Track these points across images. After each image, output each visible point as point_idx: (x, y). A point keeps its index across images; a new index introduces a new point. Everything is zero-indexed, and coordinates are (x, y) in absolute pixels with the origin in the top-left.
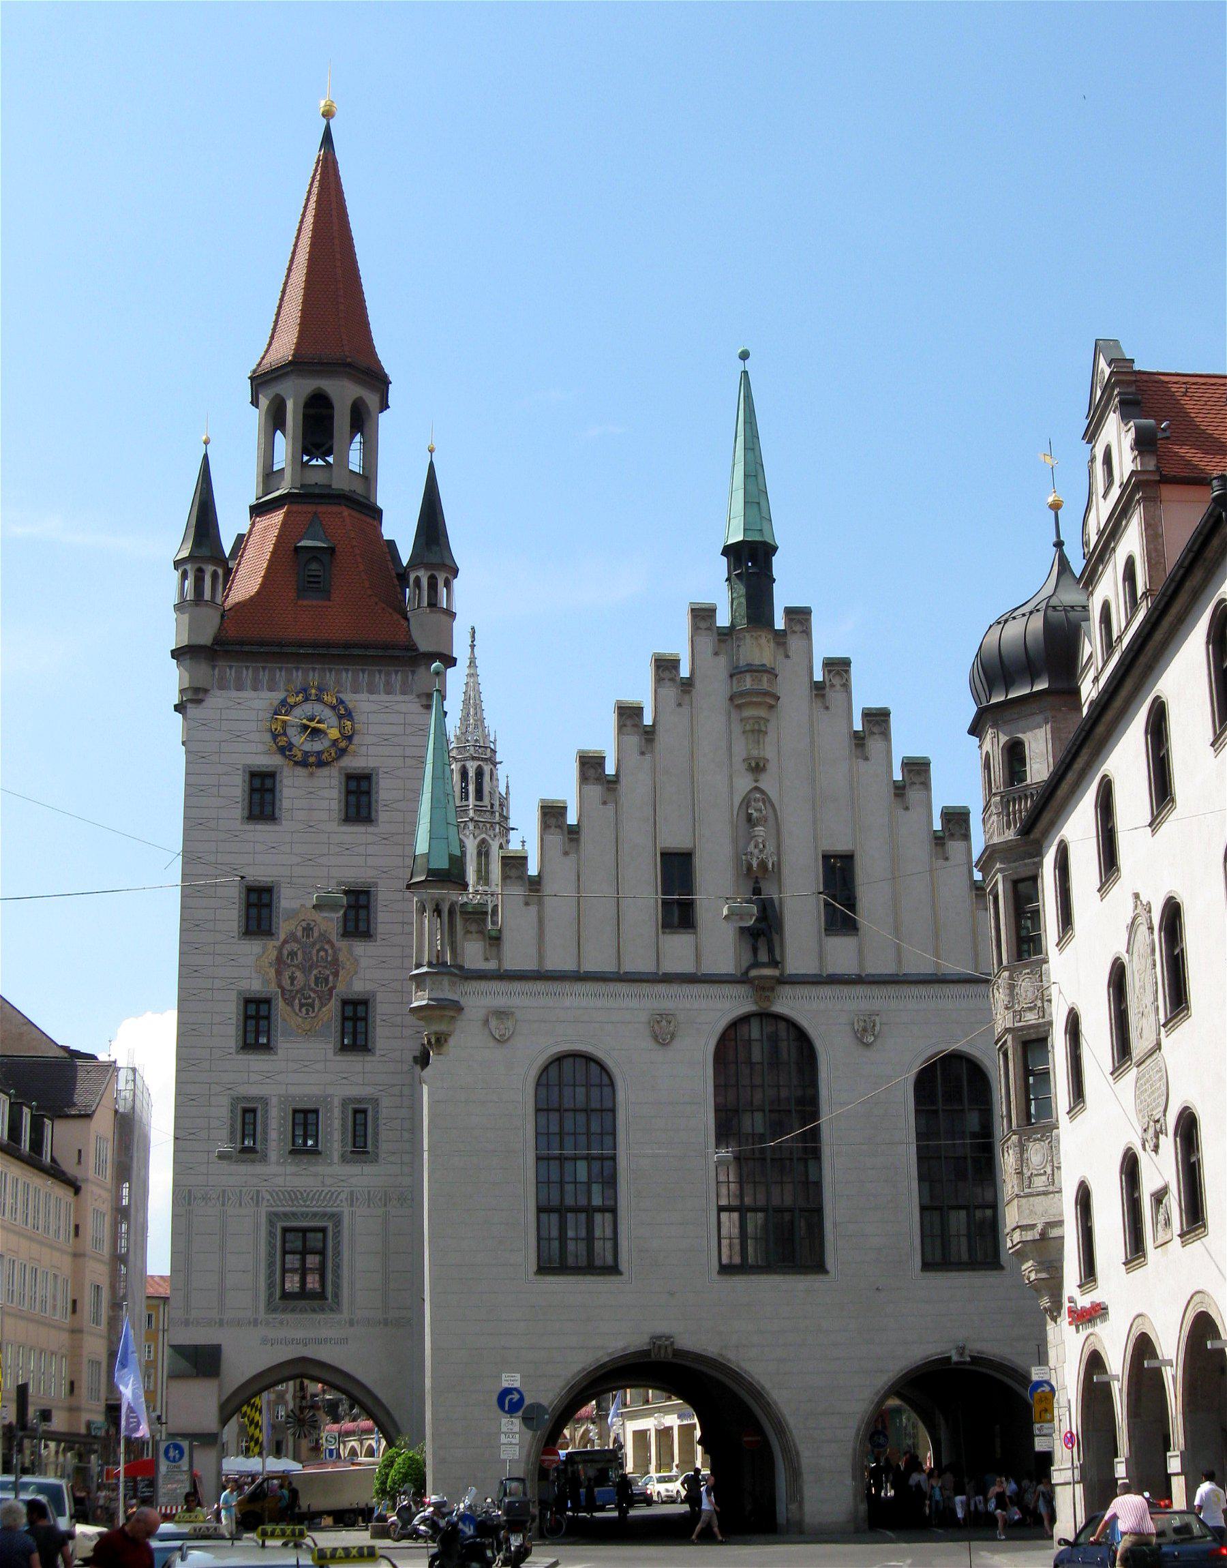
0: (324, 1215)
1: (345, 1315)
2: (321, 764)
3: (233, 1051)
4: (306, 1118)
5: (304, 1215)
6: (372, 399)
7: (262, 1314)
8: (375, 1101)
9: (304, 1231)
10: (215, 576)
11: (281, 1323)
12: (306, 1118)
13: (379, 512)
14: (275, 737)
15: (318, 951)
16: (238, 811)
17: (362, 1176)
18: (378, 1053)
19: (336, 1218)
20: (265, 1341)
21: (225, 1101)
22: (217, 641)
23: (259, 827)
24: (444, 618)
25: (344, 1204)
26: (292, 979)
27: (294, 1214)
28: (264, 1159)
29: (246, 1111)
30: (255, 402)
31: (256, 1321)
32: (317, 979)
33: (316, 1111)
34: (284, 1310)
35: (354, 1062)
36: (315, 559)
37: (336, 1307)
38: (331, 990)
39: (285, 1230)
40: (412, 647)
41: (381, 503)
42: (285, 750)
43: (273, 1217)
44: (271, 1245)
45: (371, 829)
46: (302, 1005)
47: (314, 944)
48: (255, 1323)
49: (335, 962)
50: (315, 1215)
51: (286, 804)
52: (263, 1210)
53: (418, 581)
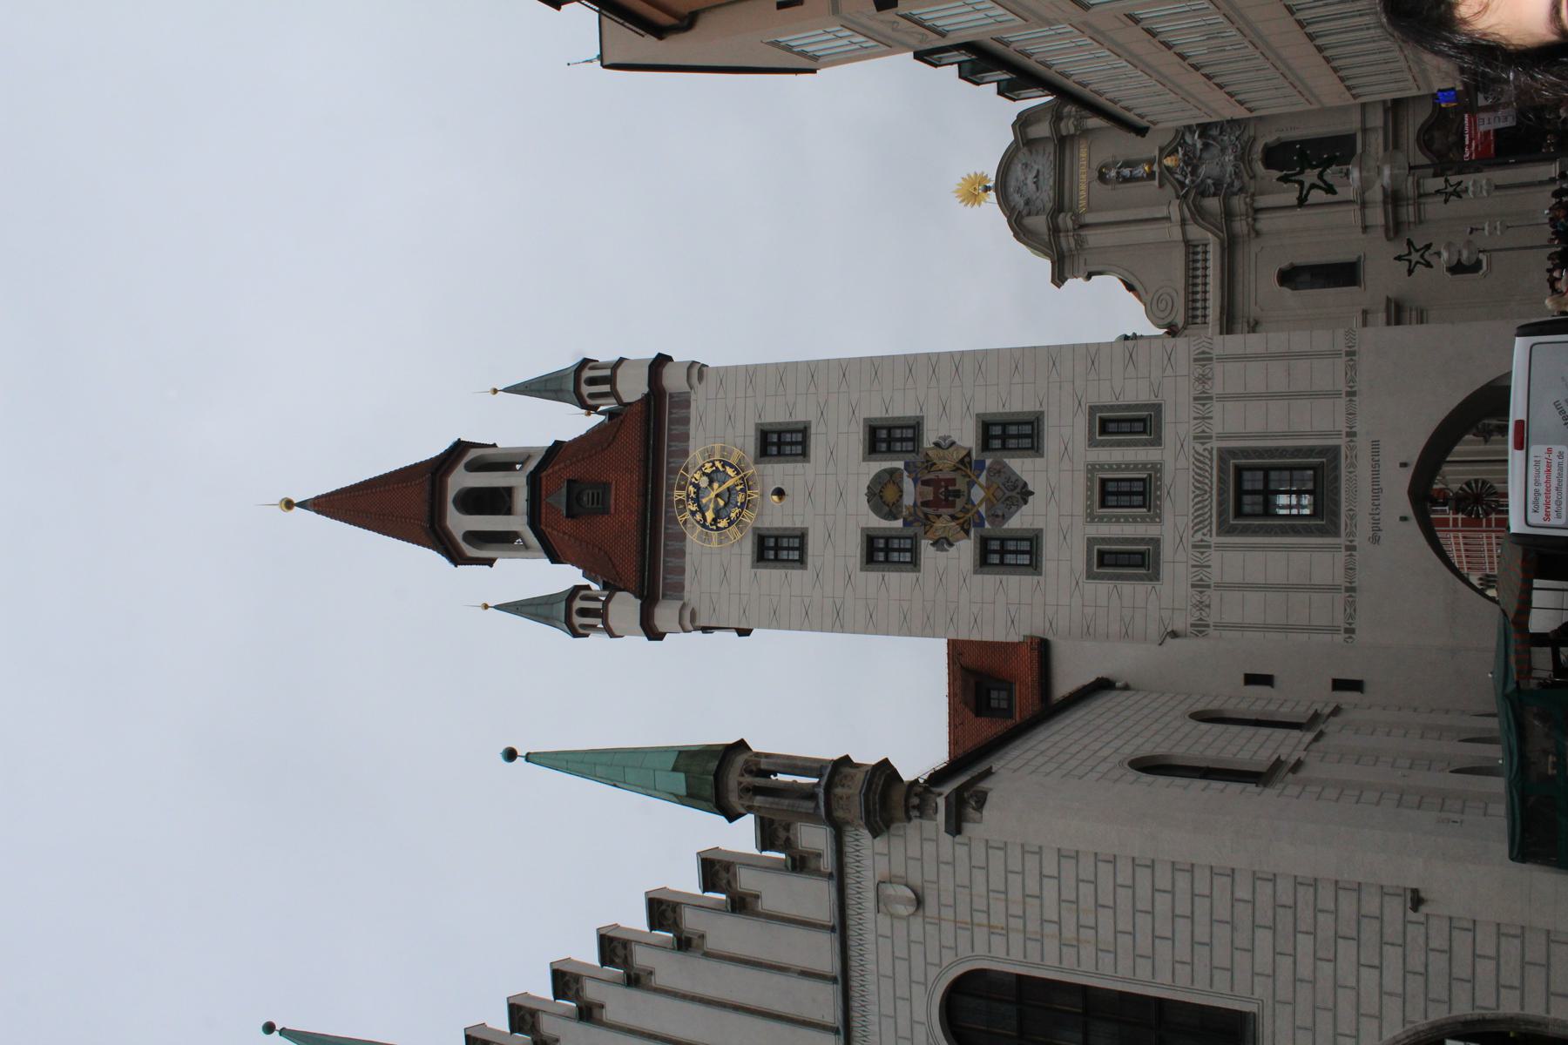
0: (1222, 470)
1: (1342, 442)
4: (1113, 494)
5: (1222, 492)
6: (472, 454)
7: (1342, 540)
9: (1240, 492)
10: (585, 598)
11: (1352, 518)
12: (1113, 494)
13: (558, 445)
16: (795, 574)
17: (1177, 425)
19: (1225, 455)
20: (1375, 540)
22: (638, 594)
23: (810, 551)
24: (620, 372)
25: (1208, 446)
27: (1220, 504)
28: (1156, 542)
29: (1101, 564)
30: (490, 562)
31: (1348, 548)
33: (1104, 482)
34: (1335, 514)
35: (1051, 441)
36: (579, 499)
37: (1334, 452)
39: (1239, 513)
40: (647, 398)
41: (550, 444)
43: (1225, 529)
44: (1255, 531)
48: (1351, 548)
50: (1220, 480)
51: (788, 524)
52: (1215, 539)
53: (592, 396)
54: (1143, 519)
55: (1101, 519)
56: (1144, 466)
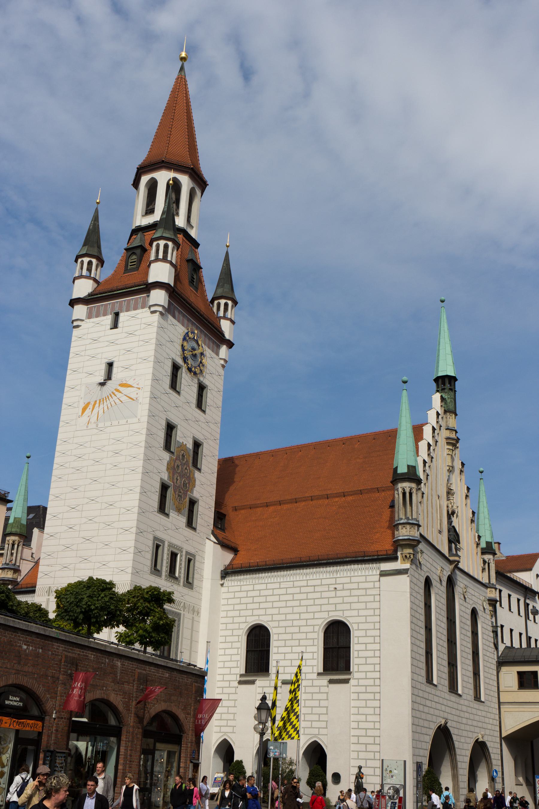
2: (195, 373)
3: (156, 510)
8: (194, 556)
14: (183, 349)
15: (186, 469)
18: (197, 531)
21: (151, 538)
26: (177, 480)
28: (160, 576)
32: (184, 483)
38: (187, 491)
42: (185, 359)
45: (203, 414)
46: (179, 496)
47: (184, 464)
49: (189, 478)
54: (166, 571)
55: (168, 550)
56: (180, 576)
